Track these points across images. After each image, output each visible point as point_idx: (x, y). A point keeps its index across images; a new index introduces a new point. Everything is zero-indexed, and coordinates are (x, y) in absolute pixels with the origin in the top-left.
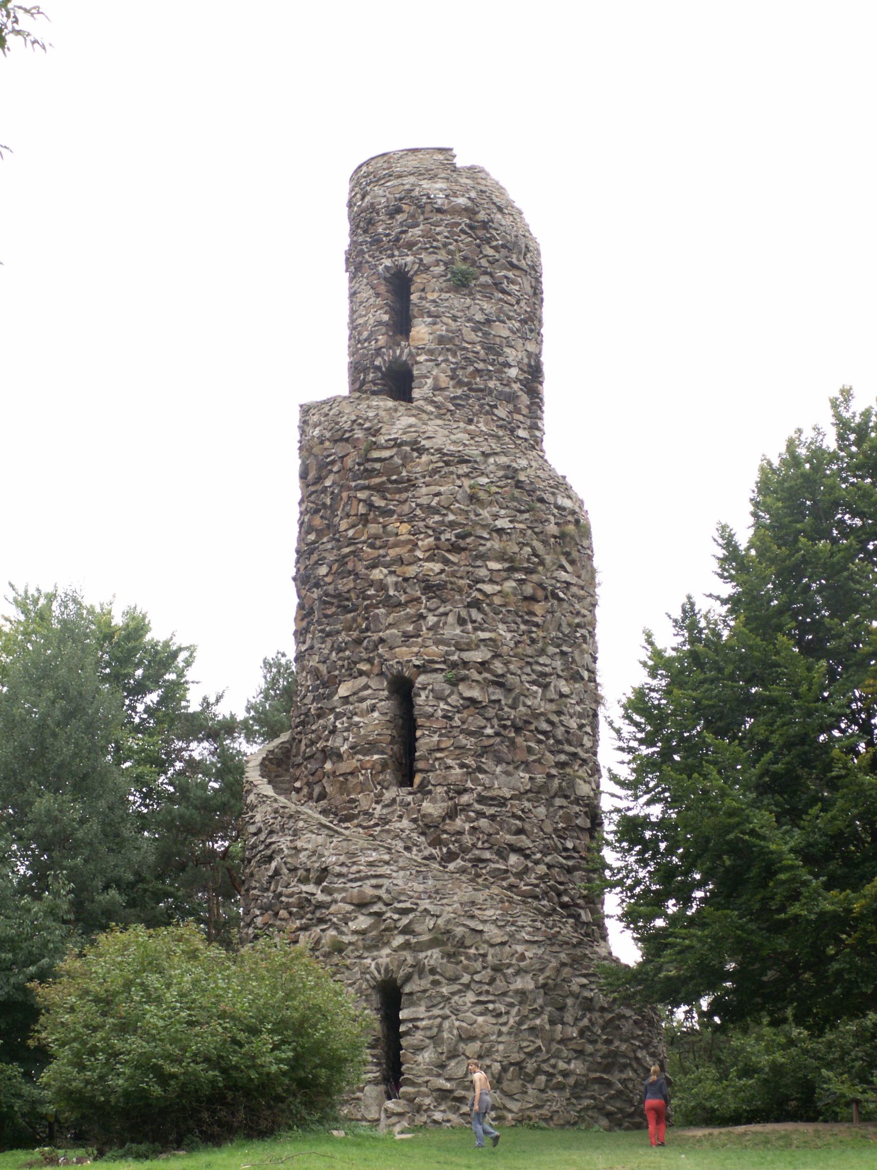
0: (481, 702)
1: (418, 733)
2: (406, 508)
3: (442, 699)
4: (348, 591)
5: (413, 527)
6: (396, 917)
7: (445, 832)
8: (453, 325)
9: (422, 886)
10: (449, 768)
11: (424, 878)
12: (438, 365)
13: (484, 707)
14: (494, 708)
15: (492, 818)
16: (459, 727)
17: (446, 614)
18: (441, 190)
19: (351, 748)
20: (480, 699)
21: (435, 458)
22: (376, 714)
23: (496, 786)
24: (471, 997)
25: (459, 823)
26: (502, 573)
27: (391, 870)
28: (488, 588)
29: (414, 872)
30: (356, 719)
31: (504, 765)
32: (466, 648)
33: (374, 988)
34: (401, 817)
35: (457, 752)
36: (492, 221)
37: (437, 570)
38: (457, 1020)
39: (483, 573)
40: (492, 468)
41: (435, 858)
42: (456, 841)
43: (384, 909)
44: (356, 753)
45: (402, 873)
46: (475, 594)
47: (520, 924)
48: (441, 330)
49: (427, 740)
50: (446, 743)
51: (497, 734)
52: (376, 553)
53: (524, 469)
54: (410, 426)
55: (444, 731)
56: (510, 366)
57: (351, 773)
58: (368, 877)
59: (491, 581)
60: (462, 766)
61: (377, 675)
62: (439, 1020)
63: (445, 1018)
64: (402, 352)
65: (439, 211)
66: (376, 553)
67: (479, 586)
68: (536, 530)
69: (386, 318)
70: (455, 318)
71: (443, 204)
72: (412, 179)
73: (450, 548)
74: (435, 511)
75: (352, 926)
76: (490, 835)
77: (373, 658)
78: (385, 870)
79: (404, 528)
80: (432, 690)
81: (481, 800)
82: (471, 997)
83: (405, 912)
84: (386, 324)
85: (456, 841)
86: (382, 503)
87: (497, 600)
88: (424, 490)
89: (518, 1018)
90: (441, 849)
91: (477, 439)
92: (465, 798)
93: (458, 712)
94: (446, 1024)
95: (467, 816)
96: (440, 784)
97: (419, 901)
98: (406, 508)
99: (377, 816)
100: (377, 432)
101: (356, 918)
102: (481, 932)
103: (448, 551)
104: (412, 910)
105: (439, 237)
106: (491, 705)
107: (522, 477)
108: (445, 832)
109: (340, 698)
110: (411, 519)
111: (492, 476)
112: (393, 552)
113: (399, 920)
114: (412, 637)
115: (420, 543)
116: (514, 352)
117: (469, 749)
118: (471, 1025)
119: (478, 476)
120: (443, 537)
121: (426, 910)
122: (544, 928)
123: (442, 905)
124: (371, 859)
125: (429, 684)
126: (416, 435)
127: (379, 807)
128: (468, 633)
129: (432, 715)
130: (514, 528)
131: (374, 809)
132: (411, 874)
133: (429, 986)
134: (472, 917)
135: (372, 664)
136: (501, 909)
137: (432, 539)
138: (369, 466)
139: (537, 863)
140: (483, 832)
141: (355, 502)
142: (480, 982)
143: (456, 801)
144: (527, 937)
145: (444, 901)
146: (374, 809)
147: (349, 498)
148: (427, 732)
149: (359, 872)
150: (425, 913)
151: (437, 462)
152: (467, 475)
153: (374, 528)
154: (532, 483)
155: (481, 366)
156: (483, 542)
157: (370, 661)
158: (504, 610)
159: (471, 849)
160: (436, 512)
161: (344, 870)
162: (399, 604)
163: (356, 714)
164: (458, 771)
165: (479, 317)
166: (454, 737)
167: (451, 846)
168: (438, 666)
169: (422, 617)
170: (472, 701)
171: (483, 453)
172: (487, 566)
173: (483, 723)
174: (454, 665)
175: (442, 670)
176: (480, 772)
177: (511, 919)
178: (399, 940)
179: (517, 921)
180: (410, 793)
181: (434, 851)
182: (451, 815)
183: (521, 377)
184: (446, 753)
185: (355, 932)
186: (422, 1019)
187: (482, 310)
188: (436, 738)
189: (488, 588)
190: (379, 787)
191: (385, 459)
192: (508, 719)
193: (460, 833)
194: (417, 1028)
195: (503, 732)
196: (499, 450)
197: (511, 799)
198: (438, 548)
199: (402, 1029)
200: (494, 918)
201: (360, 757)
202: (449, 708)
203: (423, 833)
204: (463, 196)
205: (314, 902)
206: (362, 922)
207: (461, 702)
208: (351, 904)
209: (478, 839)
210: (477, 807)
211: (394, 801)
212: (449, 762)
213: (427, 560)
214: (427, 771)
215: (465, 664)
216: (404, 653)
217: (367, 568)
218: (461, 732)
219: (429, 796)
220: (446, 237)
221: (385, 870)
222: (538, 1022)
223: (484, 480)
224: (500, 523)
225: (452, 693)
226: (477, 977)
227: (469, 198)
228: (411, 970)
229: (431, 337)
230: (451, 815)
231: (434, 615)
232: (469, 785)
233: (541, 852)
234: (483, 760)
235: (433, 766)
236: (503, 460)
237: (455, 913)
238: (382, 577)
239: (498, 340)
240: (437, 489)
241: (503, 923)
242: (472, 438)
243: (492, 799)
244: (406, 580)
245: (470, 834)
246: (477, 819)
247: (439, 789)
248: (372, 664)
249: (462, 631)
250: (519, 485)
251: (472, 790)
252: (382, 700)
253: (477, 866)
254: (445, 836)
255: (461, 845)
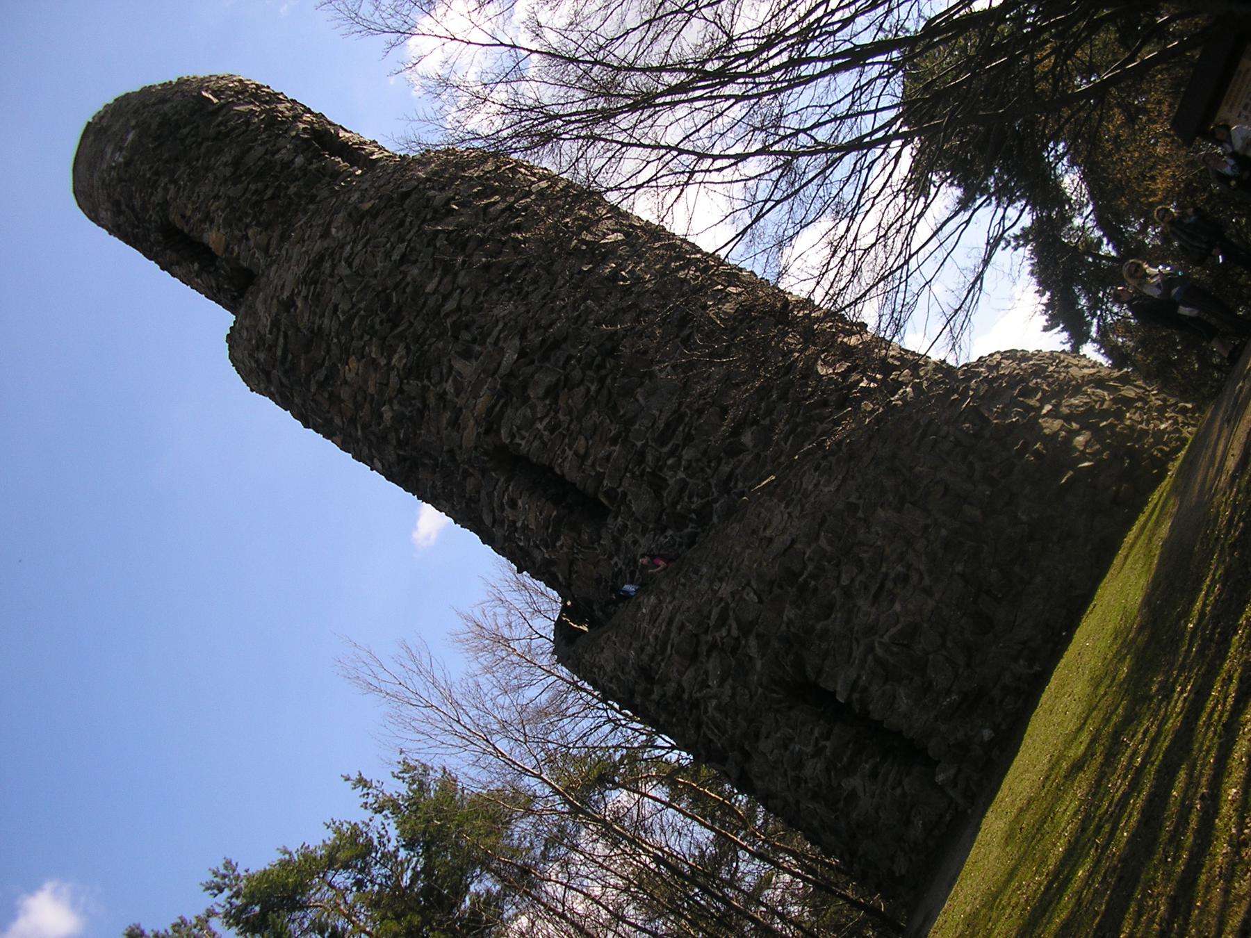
0: (559, 380)
1: (557, 470)
2: (335, 351)
3: (533, 423)
4: (398, 455)
5: (354, 353)
6: (724, 632)
7: (674, 504)
8: (222, 202)
9: (703, 580)
10: (608, 458)
11: (696, 572)
12: (247, 239)
13: (567, 379)
14: (574, 367)
15: (688, 439)
16: (571, 421)
17: (451, 368)
18: (113, 153)
19: (547, 547)
20: (554, 380)
21: (304, 293)
22: (520, 503)
23: (657, 413)
24: (863, 604)
25: (673, 479)
26: (445, 280)
27: (670, 603)
28: (451, 305)
29: (683, 580)
30: (519, 524)
31: (639, 390)
32: (495, 364)
33: (790, 708)
34: (635, 542)
35: (597, 438)
36: (166, 114)
37: (404, 353)
38: (882, 636)
39: (431, 302)
40: (341, 234)
41: (696, 535)
42: (690, 497)
43: (709, 638)
44: (554, 546)
45: (677, 594)
46: (449, 321)
47: (810, 487)
48: (219, 217)
49: (567, 465)
50: (581, 444)
51: (602, 380)
52: (367, 406)
53: (362, 200)
54: (265, 301)
55: (567, 441)
56: (292, 161)
57: (572, 563)
58: (668, 631)
59: (446, 298)
60: (614, 441)
61: (483, 477)
62: (870, 657)
63: (871, 649)
64: (223, 268)
65: (128, 163)
66: (367, 406)
67: (442, 314)
68: (428, 217)
69: (196, 266)
70: (217, 197)
71: (125, 157)
72: (96, 176)
73: (390, 324)
74: (350, 319)
75: (713, 682)
76: (705, 453)
77: (465, 471)
78: (667, 608)
79: (353, 363)
80: (519, 429)
81: (662, 440)
82: (863, 604)
83: (723, 620)
84: (202, 269)
85: (690, 497)
86: (324, 372)
87: (467, 301)
88: (326, 321)
89: (923, 558)
90: (691, 520)
91: (306, 237)
92: (649, 458)
93: (556, 412)
94: (879, 651)
95: (671, 468)
96: (621, 480)
97: (719, 594)
98: (335, 351)
99: (624, 567)
100: (261, 338)
101: (706, 672)
102: (793, 542)
103: (392, 329)
104: (726, 609)
105: (148, 176)
106: (568, 369)
107: (368, 205)
108: (674, 504)
109: (493, 526)
110: (346, 352)
111: (348, 238)
112: (372, 390)
113: (729, 631)
114: (457, 418)
115: (373, 356)
116: (284, 151)
117: (602, 422)
118: (897, 622)
119: (341, 254)
120: (377, 327)
121: (733, 594)
122: (833, 459)
123: (738, 571)
124: (647, 617)
125: (511, 429)
126: (275, 301)
127: (616, 559)
128: (481, 353)
129: (545, 444)
130: (409, 241)
131: (616, 564)
132: (684, 585)
133: (824, 646)
134: (770, 540)
135: (472, 475)
136: (780, 501)
137: (374, 339)
138: (287, 365)
139: (769, 412)
140: (698, 460)
141: (319, 398)
142: (853, 580)
143: (648, 470)
144: (832, 488)
145: (735, 564)
146: (616, 564)
147: (312, 400)
148: (560, 461)
149: (656, 637)
150: (737, 597)
151: (309, 291)
152: (334, 267)
153: (345, 393)
154: (380, 198)
155: (269, 192)
156: (404, 284)
157: (466, 474)
158: (481, 298)
159: (710, 485)
160: (350, 319)
161: (649, 650)
162: (421, 413)
163: (514, 522)
164: (617, 448)
165: (228, 171)
166: (580, 433)
167: (693, 506)
168: (497, 409)
169: (442, 396)
170: (552, 392)
171: (321, 236)
172: (429, 293)
173: (583, 389)
174: (506, 389)
175: (505, 405)
176: (633, 424)
177: (799, 496)
178: (753, 642)
179: (806, 489)
180: (616, 518)
181: (689, 530)
182: (657, 485)
183: (310, 155)
184: (592, 451)
185: (721, 684)
186: (859, 677)
187: (225, 165)
188: (569, 453)
189: (451, 305)
190: (596, 545)
191: (286, 344)
192: (593, 359)
193: (683, 486)
194: (865, 689)
195: (603, 372)
196: (328, 218)
197: (680, 404)
198: (384, 339)
199: (857, 707)
200: (786, 516)
201: (558, 544)
202: (547, 420)
203: (664, 530)
204: (128, 133)
205: (670, 701)
206: (713, 665)
207: (547, 402)
208: (687, 669)
209: (702, 470)
210: (665, 450)
211: (616, 540)
212: (603, 453)
213: (389, 358)
214: (601, 483)
215: (511, 374)
216: (470, 433)
217: (379, 424)
218: (580, 422)
219: (629, 497)
220: (150, 169)
221: (667, 608)
222: (944, 532)
223: (348, 248)
224: (396, 256)
225: (533, 408)
226: (845, 581)
227: (133, 128)
228: (791, 657)
229: (221, 230)
230: (657, 485)
231: (447, 381)
232: (639, 444)
233: (762, 399)
234: (622, 412)
235: (598, 474)
236: (340, 218)
237: (755, 562)
238: (390, 414)
239: (261, 163)
240: (330, 306)
241: (799, 508)
242: (304, 241)
243: (668, 425)
244: (401, 391)
245: (691, 476)
246: (680, 459)
247: (626, 483)
248: (472, 475)
249: (477, 359)
250: (374, 213)
251: (646, 445)
252: (507, 489)
253: (731, 489)
254: (679, 507)
255: (698, 495)
